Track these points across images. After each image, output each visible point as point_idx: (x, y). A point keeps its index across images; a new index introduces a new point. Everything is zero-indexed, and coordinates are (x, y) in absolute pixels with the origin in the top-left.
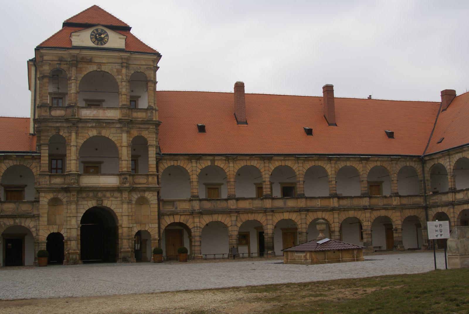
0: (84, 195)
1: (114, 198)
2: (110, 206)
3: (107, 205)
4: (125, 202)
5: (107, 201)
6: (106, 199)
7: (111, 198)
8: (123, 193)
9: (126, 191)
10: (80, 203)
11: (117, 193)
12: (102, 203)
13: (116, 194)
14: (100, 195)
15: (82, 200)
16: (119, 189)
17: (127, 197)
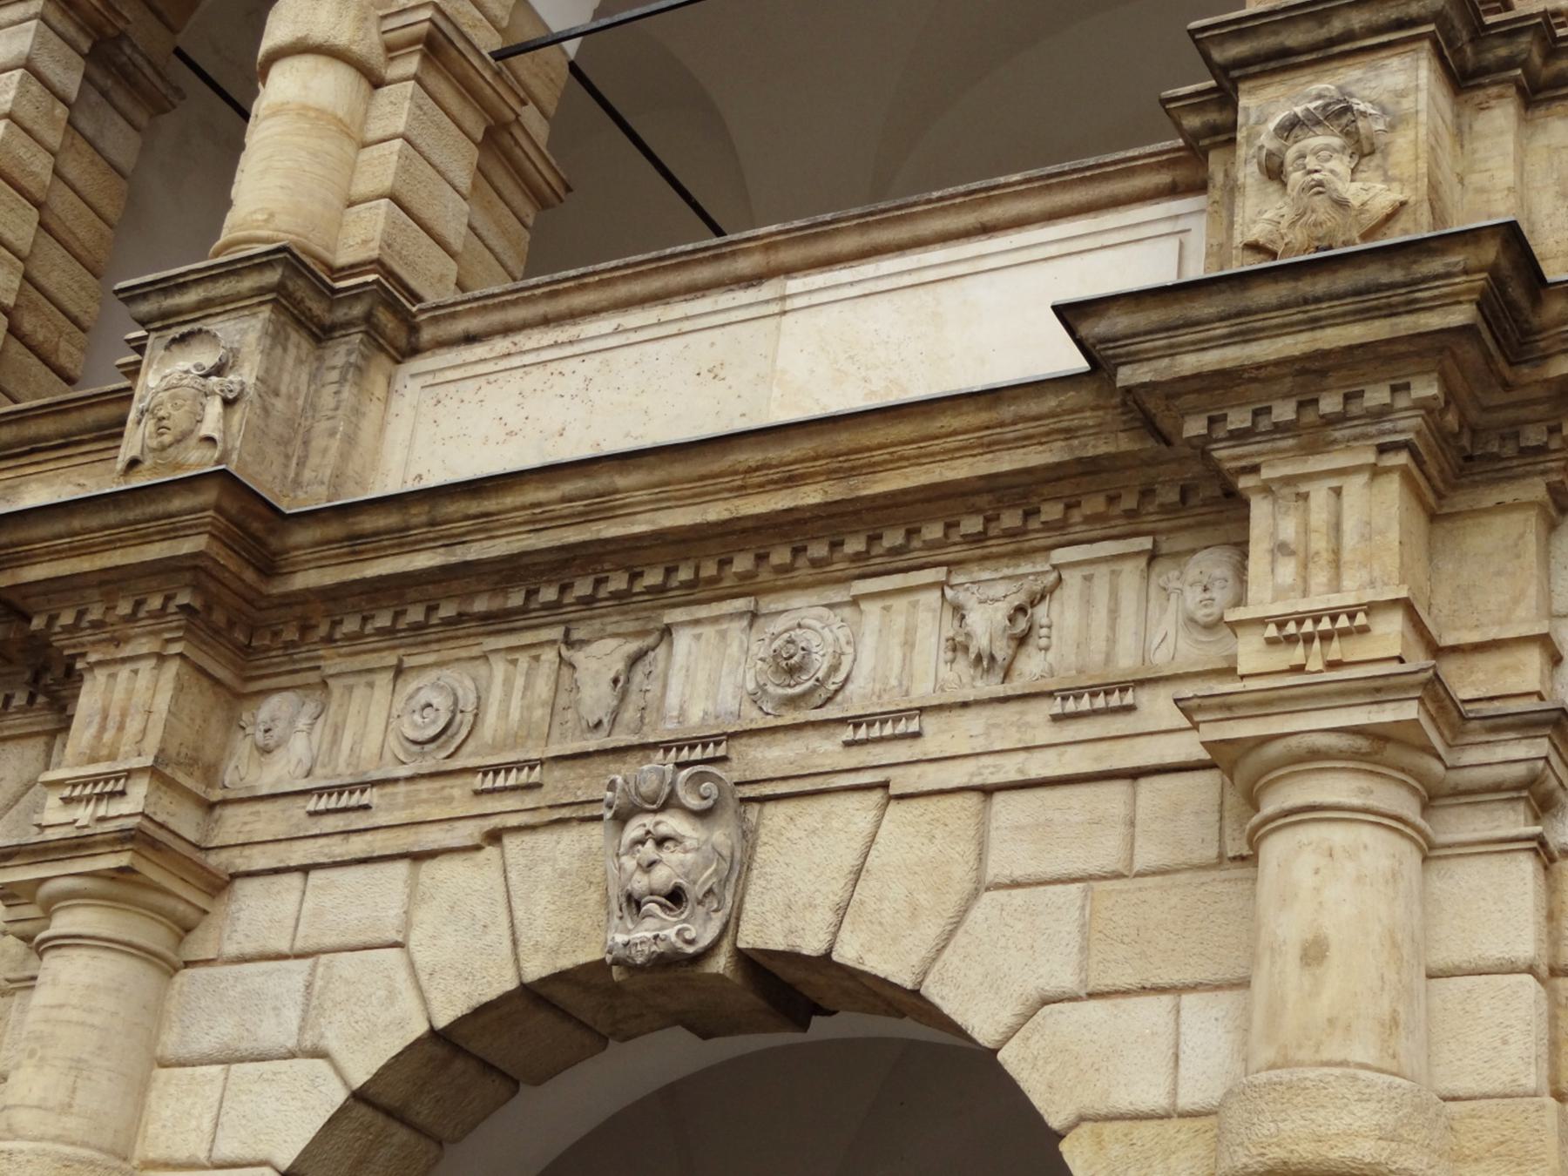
0: (369, 717)
1: (1036, 721)
2: (931, 931)
3: (842, 911)
4: (1313, 758)
5: (857, 812)
6: (826, 751)
7: (940, 736)
8: (1260, 510)
9: (1313, 435)
10: (258, 914)
11: (1131, 573)
12: (738, 869)
13: (1113, 611)
14: (707, 670)
15: (300, 854)
16: (1139, 448)
17: (1350, 622)
